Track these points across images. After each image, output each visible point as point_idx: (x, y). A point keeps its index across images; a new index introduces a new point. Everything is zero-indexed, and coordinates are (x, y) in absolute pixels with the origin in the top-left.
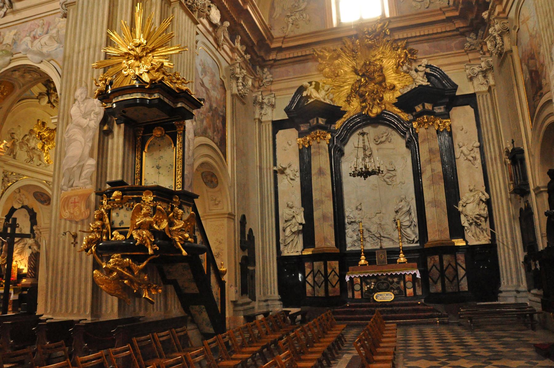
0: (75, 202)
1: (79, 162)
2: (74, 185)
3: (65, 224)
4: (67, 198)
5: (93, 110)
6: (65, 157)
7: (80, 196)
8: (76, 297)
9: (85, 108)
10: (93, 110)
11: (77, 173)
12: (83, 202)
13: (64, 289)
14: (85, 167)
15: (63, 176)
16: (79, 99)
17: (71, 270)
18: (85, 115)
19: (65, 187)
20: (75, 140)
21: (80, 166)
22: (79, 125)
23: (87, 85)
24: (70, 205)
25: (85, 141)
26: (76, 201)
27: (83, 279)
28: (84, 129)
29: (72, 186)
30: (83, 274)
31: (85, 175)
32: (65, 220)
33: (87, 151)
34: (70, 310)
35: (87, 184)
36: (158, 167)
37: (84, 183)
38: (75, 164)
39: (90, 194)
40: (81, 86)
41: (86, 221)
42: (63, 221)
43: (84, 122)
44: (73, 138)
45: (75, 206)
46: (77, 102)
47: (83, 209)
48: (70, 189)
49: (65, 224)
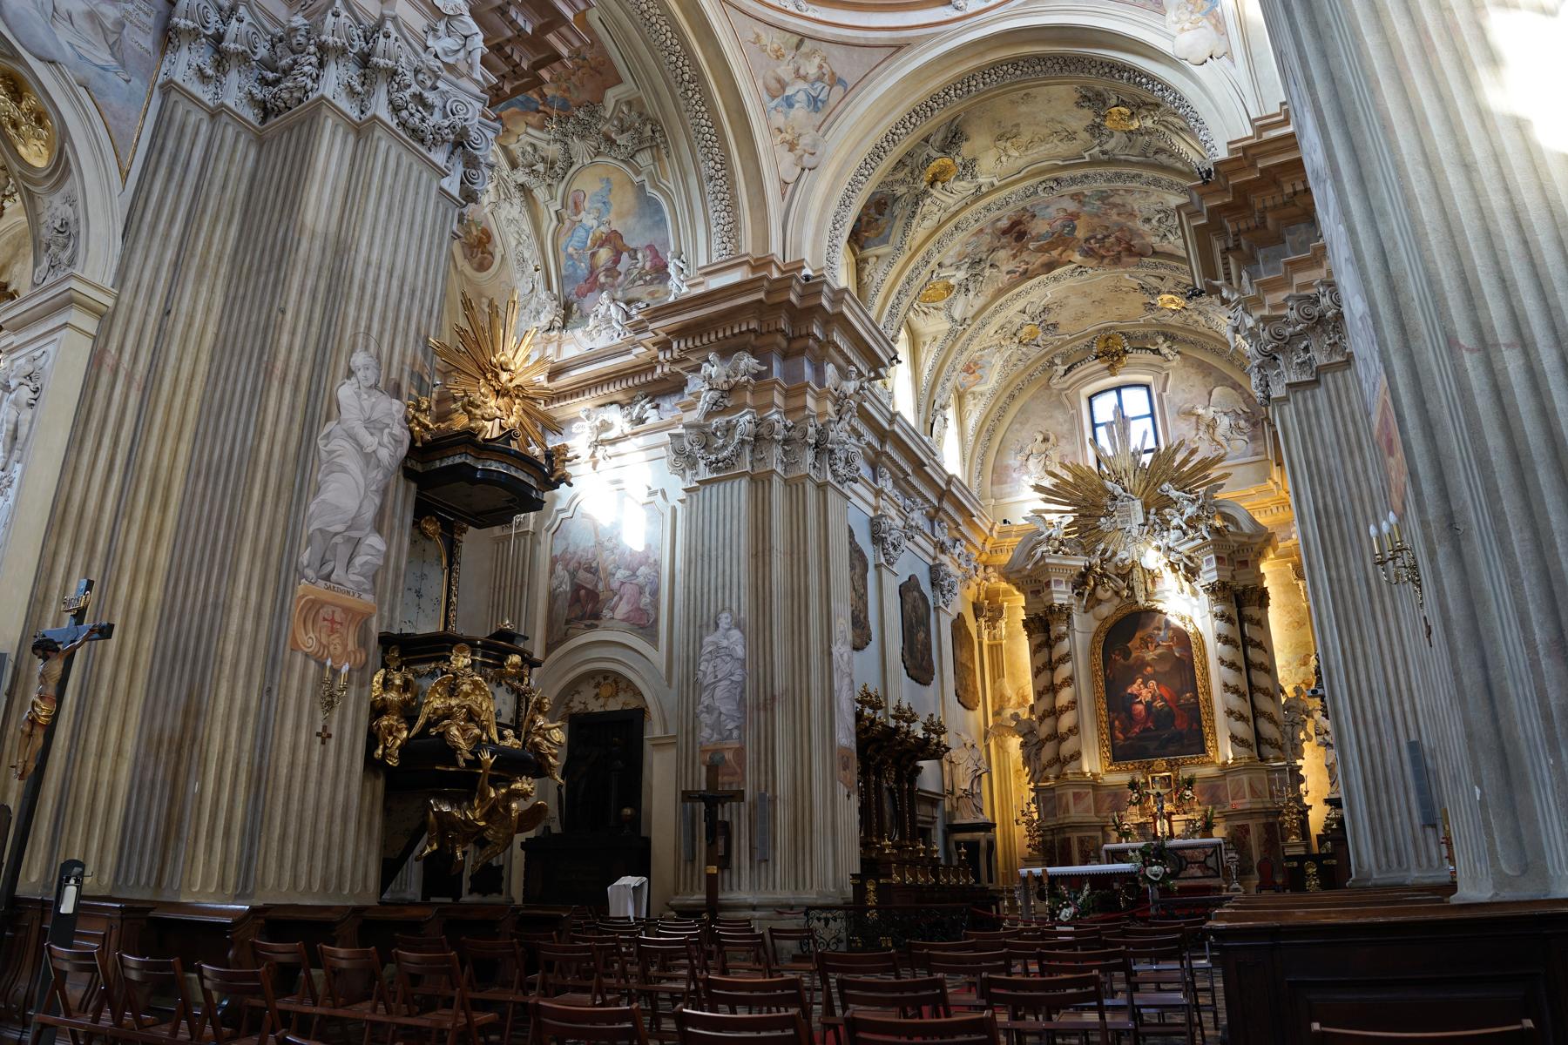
0: (333, 621)
1: (349, 528)
2: (333, 577)
3: (305, 667)
4: (313, 602)
5: (388, 426)
6: (316, 494)
7: (346, 610)
8: (320, 852)
9: (373, 408)
10: (388, 426)
11: (343, 552)
12: (352, 629)
13: (292, 830)
14: (362, 548)
15: (309, 542)
16: (360, 374)
17: (312, 786)
18: (372, 425)
19: (310, 573)
20: (343, 470)
21: (350, 539)
22: (353, 437)
23: (378, 357)
24: (320, 623)
25: (366, 487)
26: (337, 618)
27: (339, 812)
28: (368, 458)
29: (327, 578)
30: (340, 798)
31: (362, 565)
32: (306, 655)
33: (369, 513)
34: (303, 883)
35: (365, 591)
36: (419, 594)
37: (358, 584)
38: (339, 528)
39: (370, 616)
40: (366, 348)
41: (355, 675)
42: (299, 658)
43: (370, 441)
44: (338, 460)
45: (333, 631)
46: (353, 380)
47: (351, 647)
48: (322, 583)
49: (305, 667)
